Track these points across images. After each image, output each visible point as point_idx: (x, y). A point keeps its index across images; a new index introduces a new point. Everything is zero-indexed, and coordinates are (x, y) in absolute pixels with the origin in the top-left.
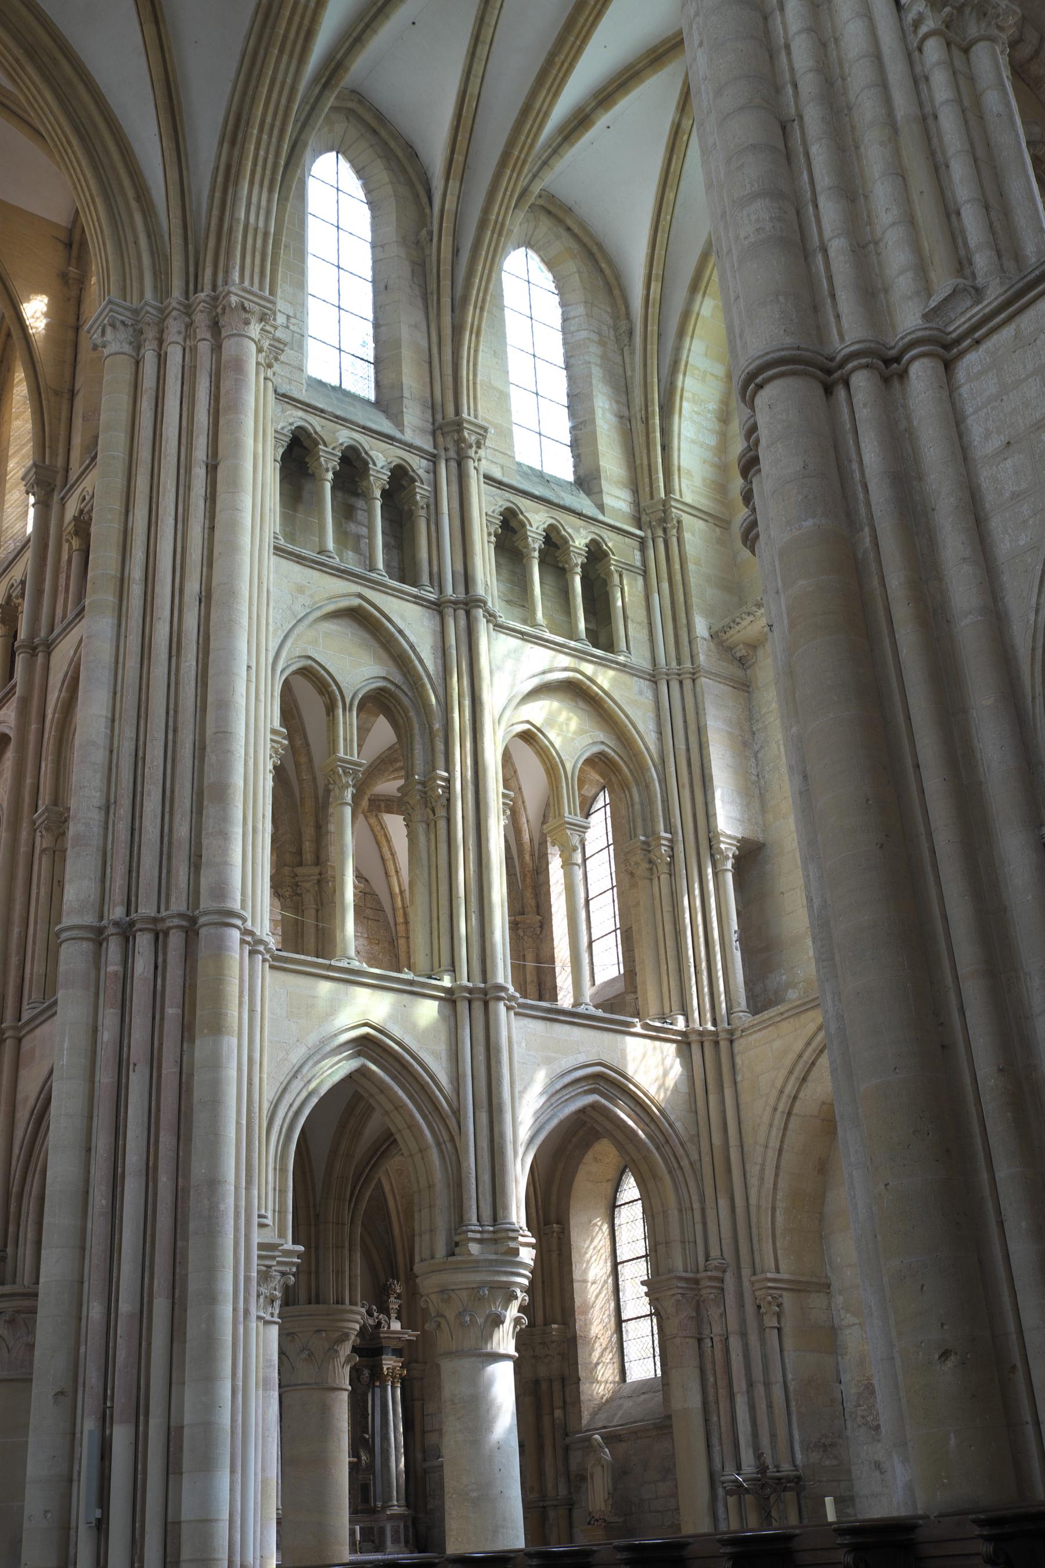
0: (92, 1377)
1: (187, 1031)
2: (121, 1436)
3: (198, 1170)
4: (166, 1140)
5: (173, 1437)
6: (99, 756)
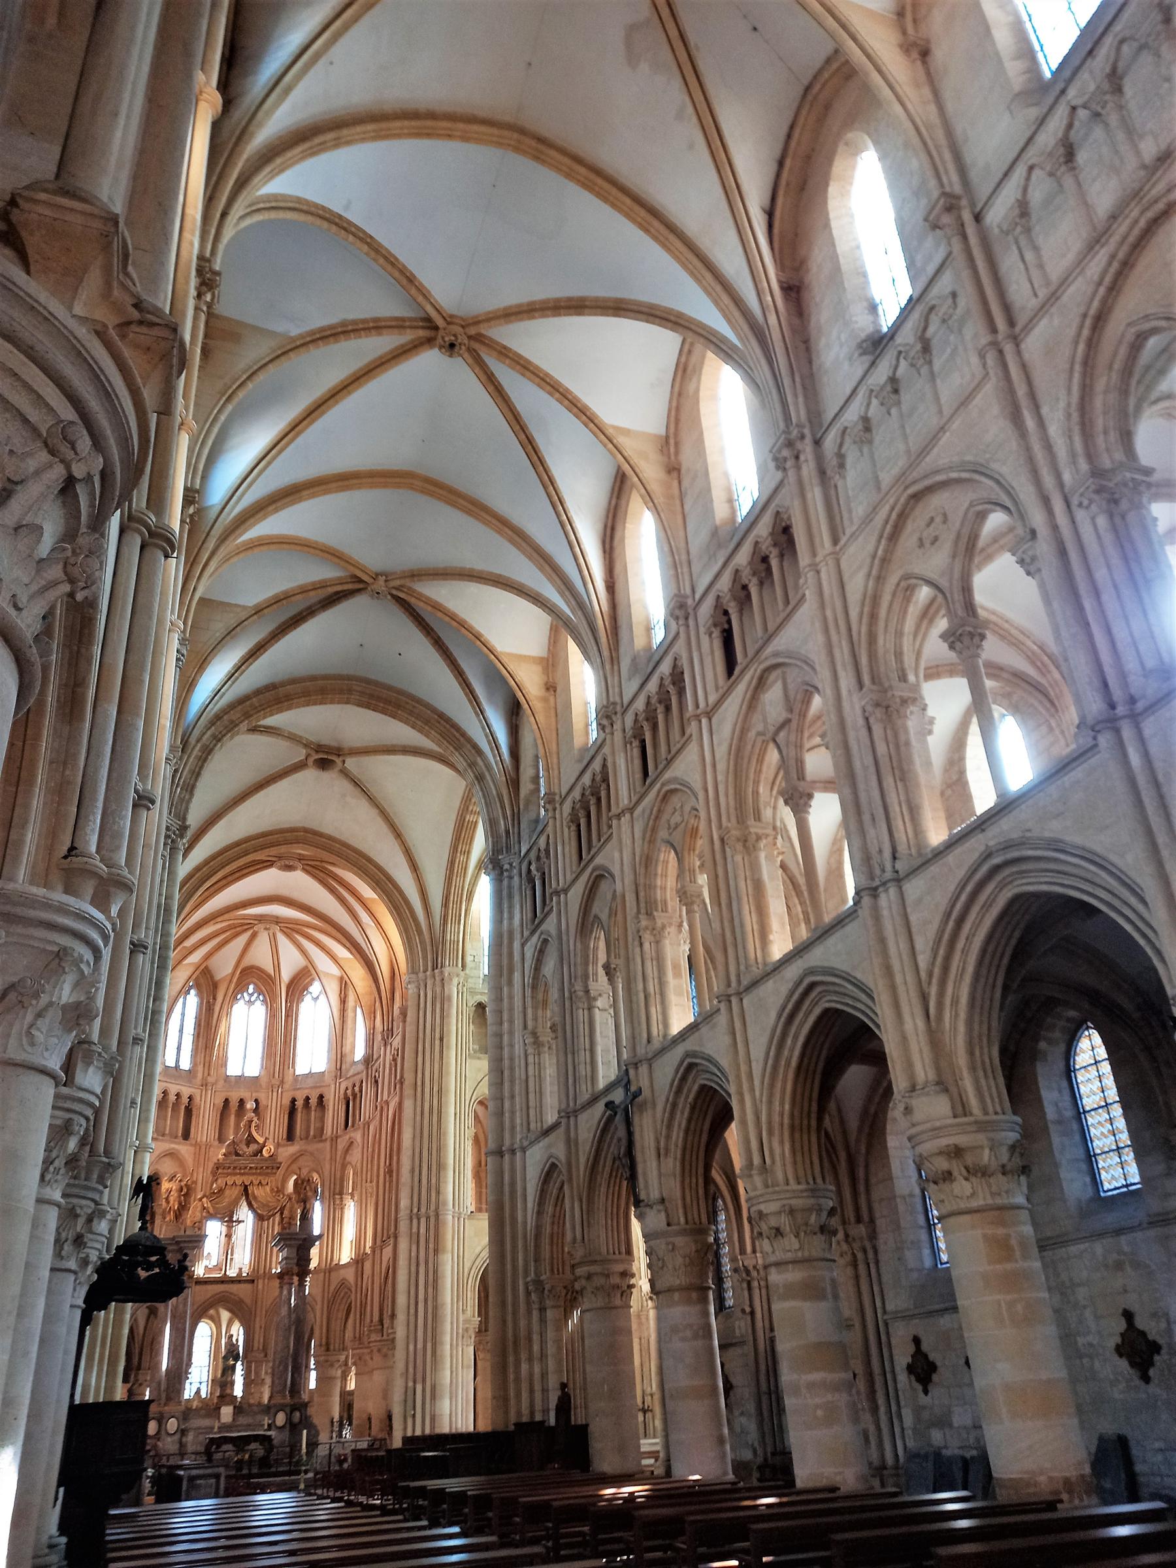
0: (411, 1370)
1: (436, 1251)
2: (419, 1388)
3: (439, 1301)
4: (430, 1290)
5: (433, 1388)
6: (410, 1153)
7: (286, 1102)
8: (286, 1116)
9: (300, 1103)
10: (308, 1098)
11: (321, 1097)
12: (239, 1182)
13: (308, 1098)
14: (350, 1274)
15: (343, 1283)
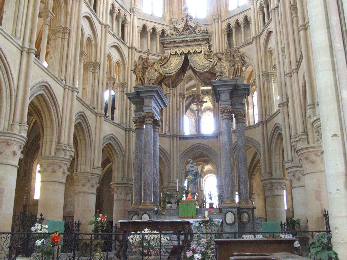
7: (224, 26)
8: (226, 36)
9: (233, 24)
10: (237, 22)
11: (246, 19)
12: (179, 52)
13: (237, 22)
14: (279, 119)
15: (277, 128)
